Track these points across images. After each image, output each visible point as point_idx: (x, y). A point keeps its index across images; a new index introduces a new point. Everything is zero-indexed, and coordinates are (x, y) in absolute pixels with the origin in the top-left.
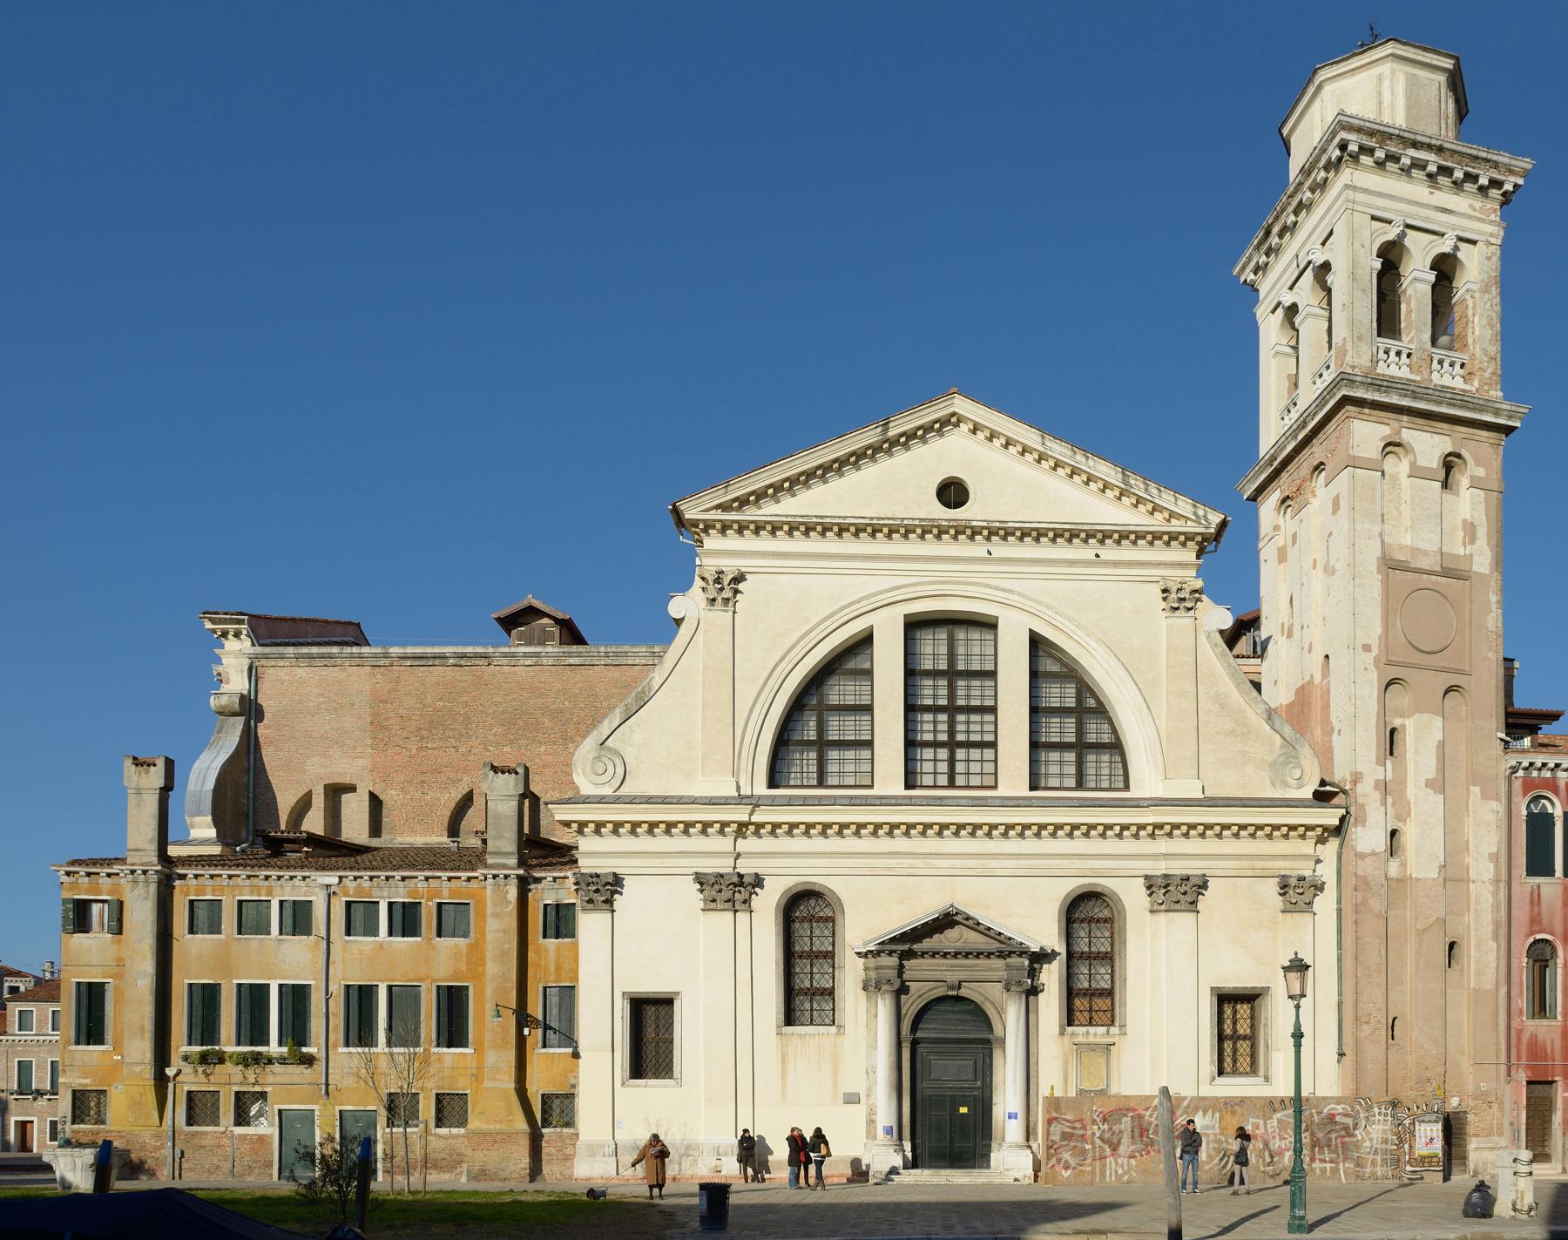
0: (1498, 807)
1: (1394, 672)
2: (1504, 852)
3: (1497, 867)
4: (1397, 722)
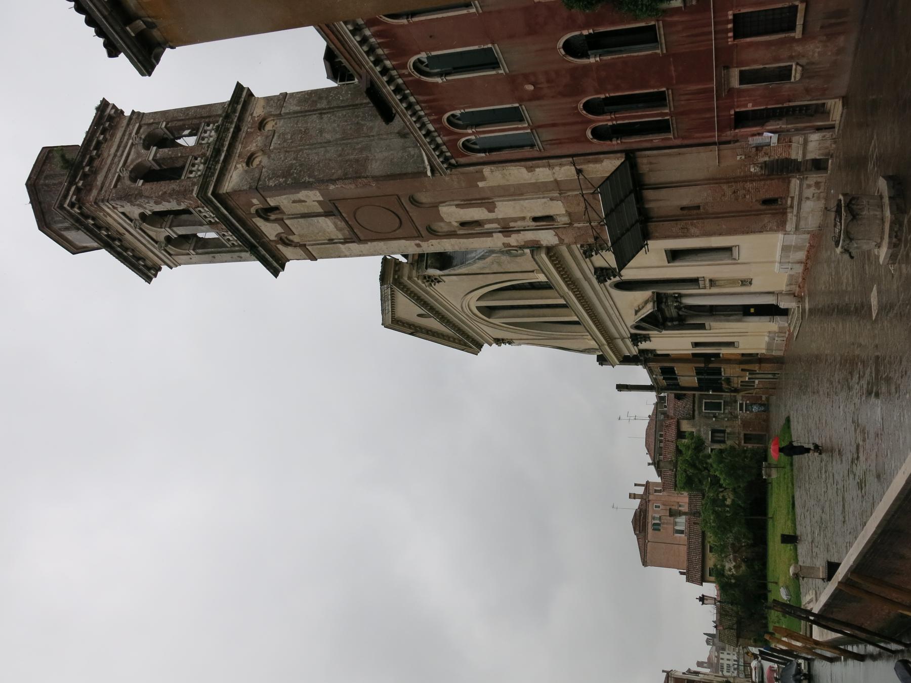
0: (486, 170)
1: (424, 232)
2: (523, 163)
3: (538, 167)
4: (456, 224)
